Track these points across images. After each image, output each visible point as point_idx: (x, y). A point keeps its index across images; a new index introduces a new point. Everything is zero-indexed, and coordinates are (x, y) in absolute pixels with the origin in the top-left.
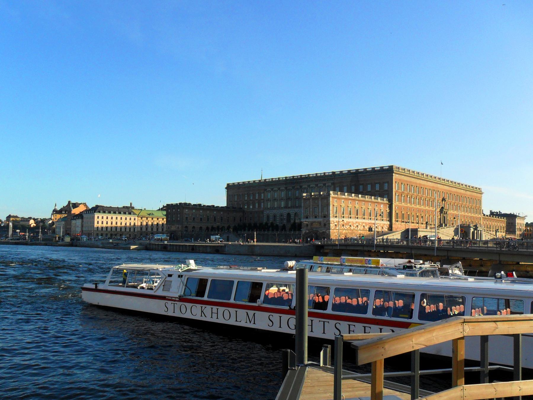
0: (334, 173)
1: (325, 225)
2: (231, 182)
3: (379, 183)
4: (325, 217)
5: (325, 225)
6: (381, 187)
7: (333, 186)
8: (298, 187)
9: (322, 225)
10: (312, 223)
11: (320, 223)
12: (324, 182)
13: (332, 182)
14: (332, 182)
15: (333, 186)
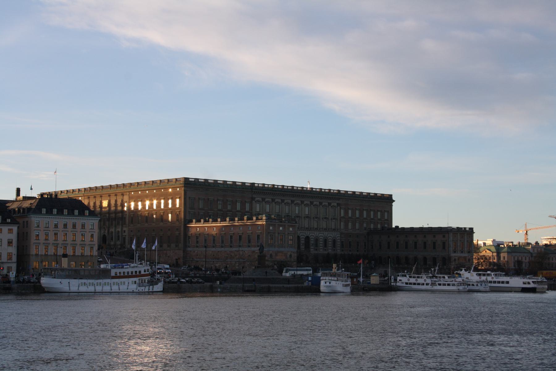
0: (339, 191)
1: (469, 260)
2: (193, 175)
3: (381, 211)
4: (469, 252)
5: (469, 260)
6: (383, 216)
7: (339, 207)
8: (299, 202)
9: (467, 260)
10: (459, 258)
11: (465, 258)
12: (293, 199)
13: (337, 202)
14: (337, 202)
15: (339, 207)
